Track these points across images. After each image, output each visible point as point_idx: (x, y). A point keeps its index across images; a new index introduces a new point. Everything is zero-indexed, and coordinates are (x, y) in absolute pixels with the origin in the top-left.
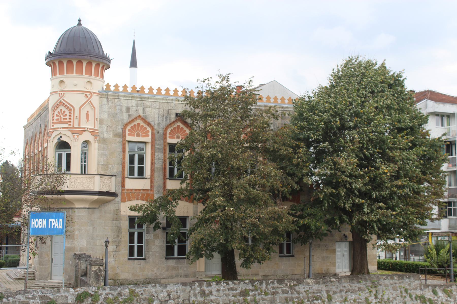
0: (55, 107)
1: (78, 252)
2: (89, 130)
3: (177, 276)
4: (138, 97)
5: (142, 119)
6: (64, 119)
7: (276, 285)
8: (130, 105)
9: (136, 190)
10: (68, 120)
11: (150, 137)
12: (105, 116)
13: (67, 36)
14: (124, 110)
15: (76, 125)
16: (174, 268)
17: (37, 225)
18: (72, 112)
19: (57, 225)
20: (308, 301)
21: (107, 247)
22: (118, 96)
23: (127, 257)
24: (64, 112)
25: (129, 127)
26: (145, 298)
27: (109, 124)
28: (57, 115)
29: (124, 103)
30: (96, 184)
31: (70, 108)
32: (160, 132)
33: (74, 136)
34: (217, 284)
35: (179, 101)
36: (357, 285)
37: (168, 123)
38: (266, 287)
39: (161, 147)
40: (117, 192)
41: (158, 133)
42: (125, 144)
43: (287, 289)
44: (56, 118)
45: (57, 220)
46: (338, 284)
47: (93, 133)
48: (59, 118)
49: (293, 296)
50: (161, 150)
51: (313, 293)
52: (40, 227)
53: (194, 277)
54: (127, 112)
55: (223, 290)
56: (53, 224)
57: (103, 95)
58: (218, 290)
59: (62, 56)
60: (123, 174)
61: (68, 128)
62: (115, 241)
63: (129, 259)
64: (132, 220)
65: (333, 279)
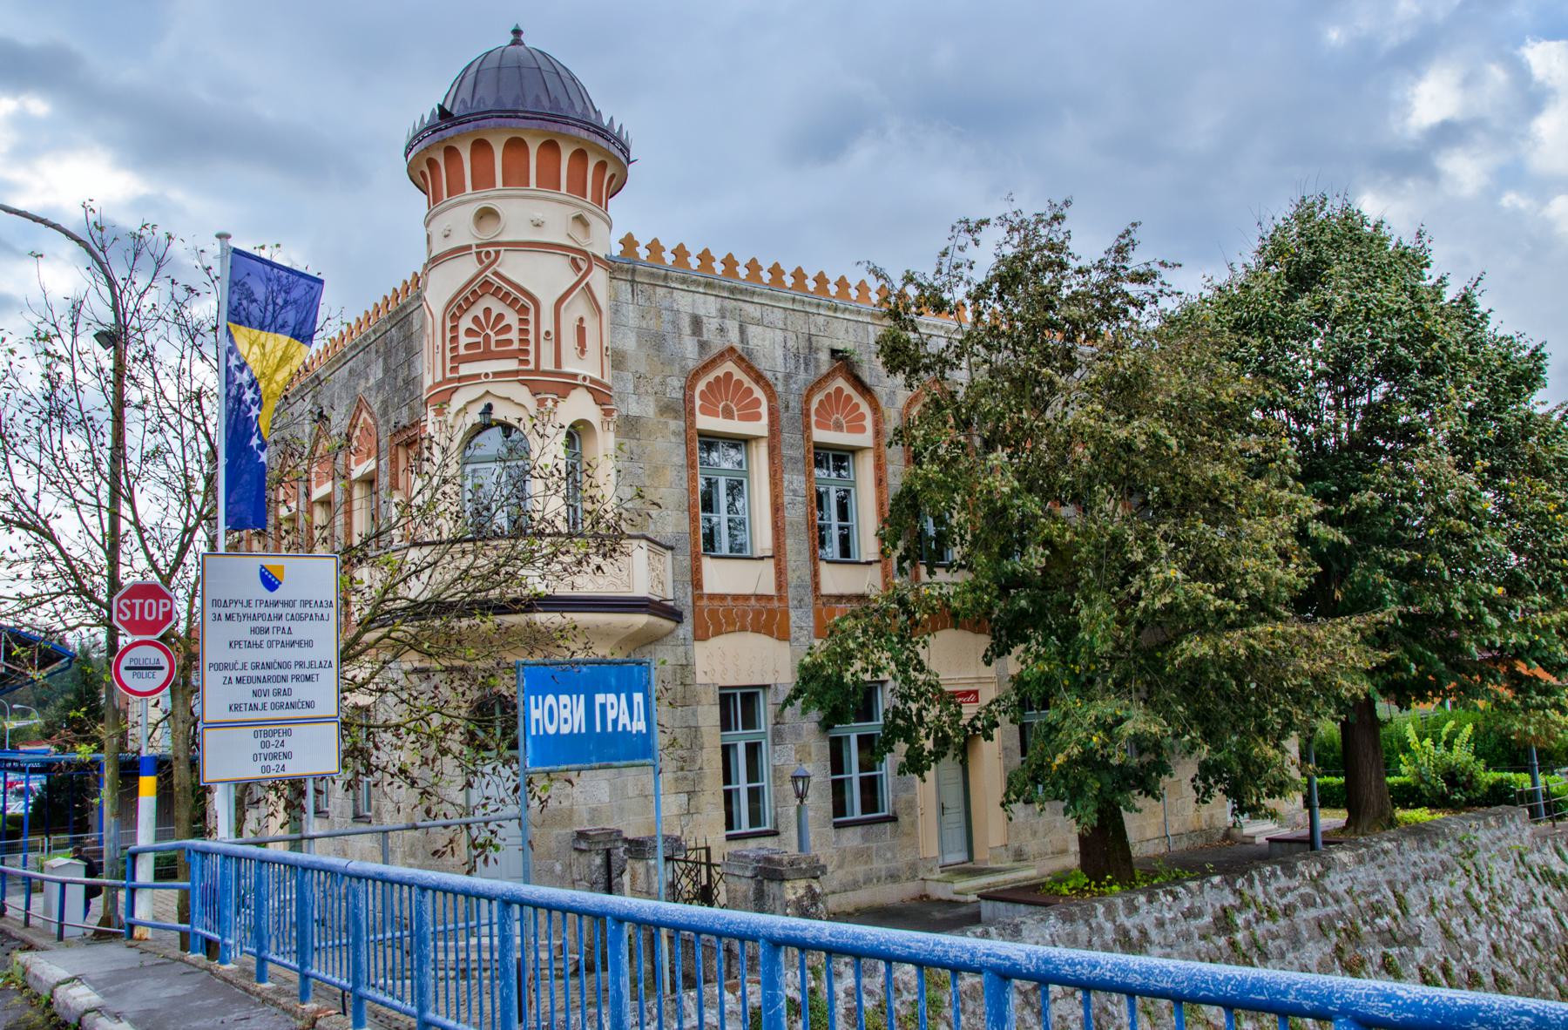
0: (459, 305)
1: (586, 827)
2: (587, 383)
3: (868, 881)
4: (723, 288)
5: (741, 358)
6: (498, 343)
7: (1284, 881)
8: (701, 312)
9: (736, 597)
10: (516, 346)
11: (765, 420)
12: (629, 343)
13: (493, 62)
14: (686, 324)
15: (547, 364)
16: (862, 855)
17: (551, 722)
18: (531, 317)
19: (624, 719)
20: (1365, 922)
21: (801, 796)
22: (666, 277)
23: (723, 833)
24: (500, 317)
25: (701, 386)
26: (973, 986)
27: (642, 370)
28: (469, 332)
29: (687, 302)
30: (639, 572)
31: (522, 301)
32: (792, 404)
33: (541, 403)
34: (1150, 901)
35: (836, 310)
36: (1431, 854)
37: (812, 377)
38: (1266, 893)
39: (798, 453)
40: (679, 606)
41: (787, 407)
42: (693, 440)
43: (1309, 890)
44: (464, 340)
45: (623, 696)
46: (1399, 858)
47: (600, 394)
48: (480, 339)
49: (1329, 910)
50: (800, 465)
51: (1365, 893)
52: (565, 730)
53: (914, 877)
54: (694, 334)
55: (1174, 921)
56: (611, 715)
57: (621, 269)
58: (1160, 924)
59: (492, 122)
60: (696, 544)
61: (517, 373)
62: (686, 778)
63: (729, 838)
64: (726, 698)
65: (1387, 845)
